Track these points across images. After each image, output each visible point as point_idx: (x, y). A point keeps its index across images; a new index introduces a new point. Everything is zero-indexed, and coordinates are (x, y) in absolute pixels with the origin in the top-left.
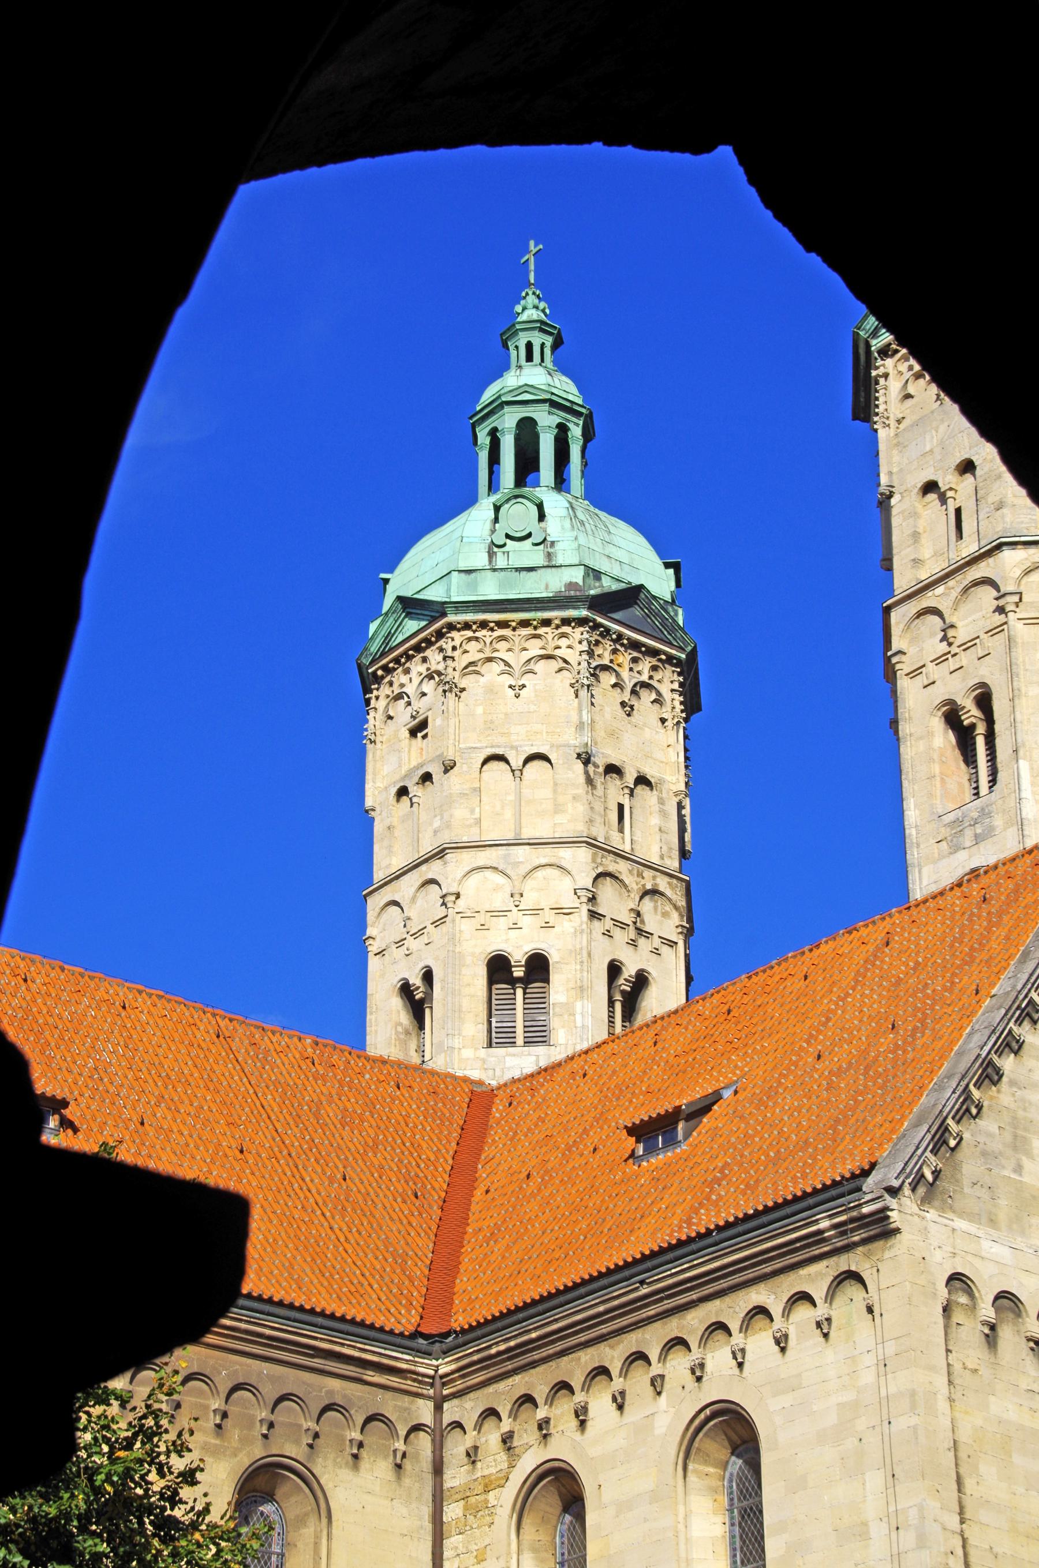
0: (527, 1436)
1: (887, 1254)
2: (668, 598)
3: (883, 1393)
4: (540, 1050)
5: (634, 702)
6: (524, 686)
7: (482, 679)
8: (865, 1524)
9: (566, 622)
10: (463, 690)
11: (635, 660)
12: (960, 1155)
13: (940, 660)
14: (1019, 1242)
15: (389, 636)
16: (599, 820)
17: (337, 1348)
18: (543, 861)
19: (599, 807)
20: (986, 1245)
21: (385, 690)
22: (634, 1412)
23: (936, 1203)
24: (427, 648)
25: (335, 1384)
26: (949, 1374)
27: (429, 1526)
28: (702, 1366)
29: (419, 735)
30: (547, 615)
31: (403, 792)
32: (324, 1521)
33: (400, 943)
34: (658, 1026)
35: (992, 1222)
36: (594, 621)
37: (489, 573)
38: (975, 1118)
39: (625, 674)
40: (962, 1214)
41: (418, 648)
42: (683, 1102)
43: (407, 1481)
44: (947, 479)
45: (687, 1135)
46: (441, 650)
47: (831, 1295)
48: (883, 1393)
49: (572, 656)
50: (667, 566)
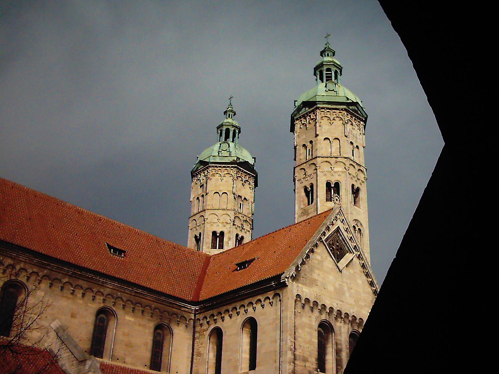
0: (212, 322)
2: (253, 164)
6: (223, 179)
7: (215, 177)
8: (276, 340)
9: (232, 167)
11: (245, 175)
12: (301, 272)
13: (303, 178)
14: (311, 289)
16: (236, 206)
23: (295, 281)
25: (175, 310)
27: (192, 337)
30: (229, 165)
32: (172, 335)
34: (244, 245)
35: (306, 285)
36: (238, 167)
38: (304, 264)
39: (243, 178)
43: (188, 329)
45: (248, 266)
50: (253, 158)
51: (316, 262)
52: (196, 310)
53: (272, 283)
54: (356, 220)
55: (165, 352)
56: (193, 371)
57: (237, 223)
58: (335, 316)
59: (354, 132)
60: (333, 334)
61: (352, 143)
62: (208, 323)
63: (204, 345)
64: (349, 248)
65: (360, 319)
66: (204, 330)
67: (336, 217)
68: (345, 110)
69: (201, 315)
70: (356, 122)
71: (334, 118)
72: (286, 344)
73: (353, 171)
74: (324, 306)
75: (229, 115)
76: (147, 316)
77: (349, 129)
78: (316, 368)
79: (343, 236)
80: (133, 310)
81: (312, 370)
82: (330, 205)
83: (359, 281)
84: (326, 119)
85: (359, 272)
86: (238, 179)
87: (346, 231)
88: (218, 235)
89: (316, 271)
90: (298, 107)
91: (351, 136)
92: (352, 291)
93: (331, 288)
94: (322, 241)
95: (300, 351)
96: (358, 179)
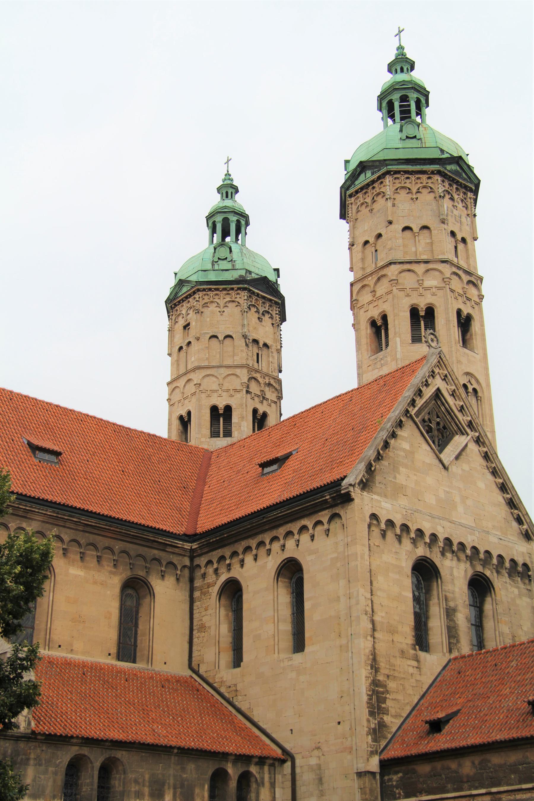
0: (223, 569)
1: (349, 507)
2: (275, 281)
3: (346, 554)
4: (229, 439)
5: (263, 317)
6: (224, 311)
7: (209, 309)
8: (339, 597)
10: (202, 312)
13: (369, 303)
15: (177, 293)
16: (250, 358)
17: (157, 539)
18: (230, 373)
19: (250, 354)
20: (384, 504)
21: (175, 313)
22: (260, 562)
23: (367, 489)
24: (190, 298)
25: (156, 552)
26: (369, 547)
27: (188, 598)
28: (284, 546)
29: (187, 328)
31: (181, 348)
32: (152, 597)
33: (179, 401)
35: (386, 496)
37: (212, 271)
40: (375, 493)
41: (186, 298)
42: (279, 455)
43: (181, 584)
44: (372, 240)
46: (195, 298)
47: (330, 521)
48: (346, 554)
49: (241, 301)
51: (402, 454)
52: (192, 550)
53: (325, 496)
54: (467, 374)
55: (141, 627)
56: (194, 659)
57: (254, 388)
58: (441, 550)
59: (455, 212)
60: (439, 580)
61: (453, 234)
62: (216, 571)
63: (210, 612)
64: (460, 425)
65: (487, 552)
66: (209, 586)
67: (433, 372)
68: (439, 173)
69: (202, 559)
70: (458, 195)
71: (419, 189)
72: (358, 603)
73: (456, 284)
74: (420, 532)
75: (227, 193)
76: (108, 566)
77: (447, 207)
78: (413, 645)
79: (446, 405)
80: (81, 557)
81: (404, 647)
82: (421, 349)
83: (481, 485)
84: (403, 193)
85: (479, 468)
86: (250, 309)
87: (453, 395)
88: (221, 412)
89: (402, 470)
90: (353, 173)
91: (451, 220)
92: (469, 502)
93: (430, 499)
94: (411, 417)
95: (383, 614)
96: (469, 299)
